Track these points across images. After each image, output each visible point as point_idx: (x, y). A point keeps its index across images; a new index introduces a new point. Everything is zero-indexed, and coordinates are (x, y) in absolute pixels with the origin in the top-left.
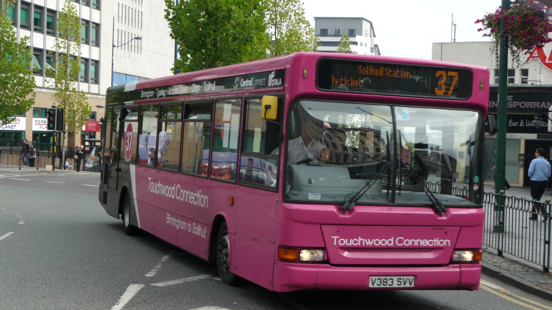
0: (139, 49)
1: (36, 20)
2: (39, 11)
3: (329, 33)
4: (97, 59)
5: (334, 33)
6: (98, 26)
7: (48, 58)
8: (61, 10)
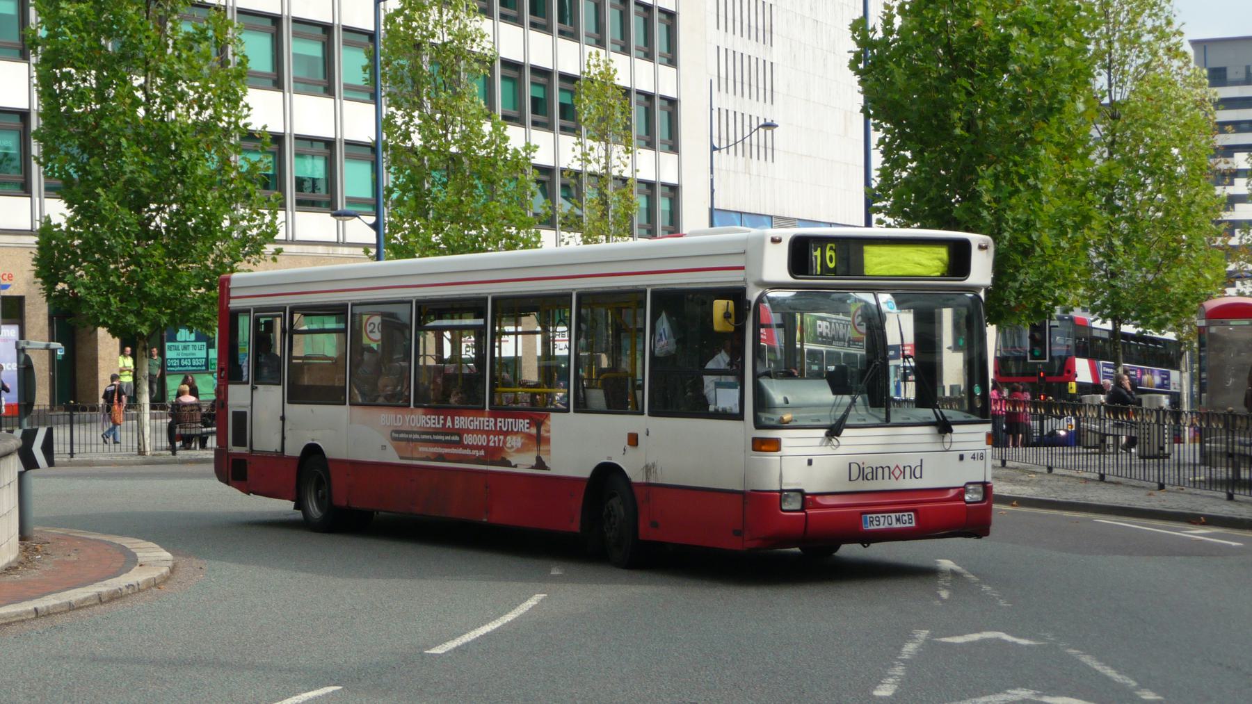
0: (769, 152)
1: (535, 101)
2: (541, 80)
3: (1231, 75)
4: (674, 181)
5: (1242, 76)
6: (672, 103)
7: (565, 187)
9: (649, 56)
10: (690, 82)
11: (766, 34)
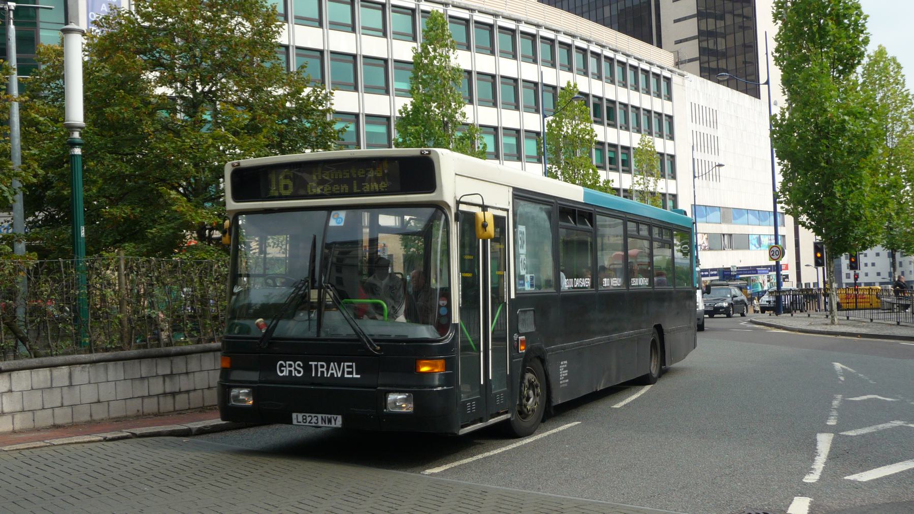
0: (718, 178)
1: (610, 159)
2: (613, 149)
4: (674, 192)
6: (672, 157)
8: (636, 146)
9: (661, 136)
10: (680, 147)
11: (715, 124)
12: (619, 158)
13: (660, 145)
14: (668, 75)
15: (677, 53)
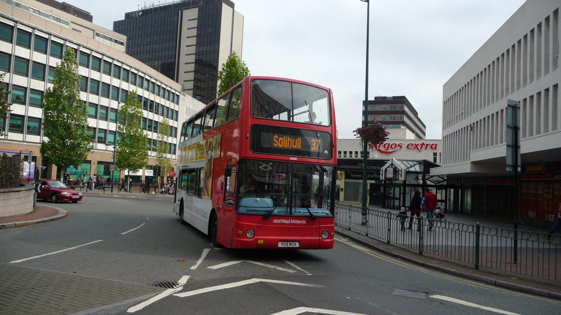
1: (149, 126)
7: (154, 143)
8: (160, 121)
9: (172, 119)
12: (153, 126)
13: (171, 123)
14: (178, 94)
15: (183, 86)
